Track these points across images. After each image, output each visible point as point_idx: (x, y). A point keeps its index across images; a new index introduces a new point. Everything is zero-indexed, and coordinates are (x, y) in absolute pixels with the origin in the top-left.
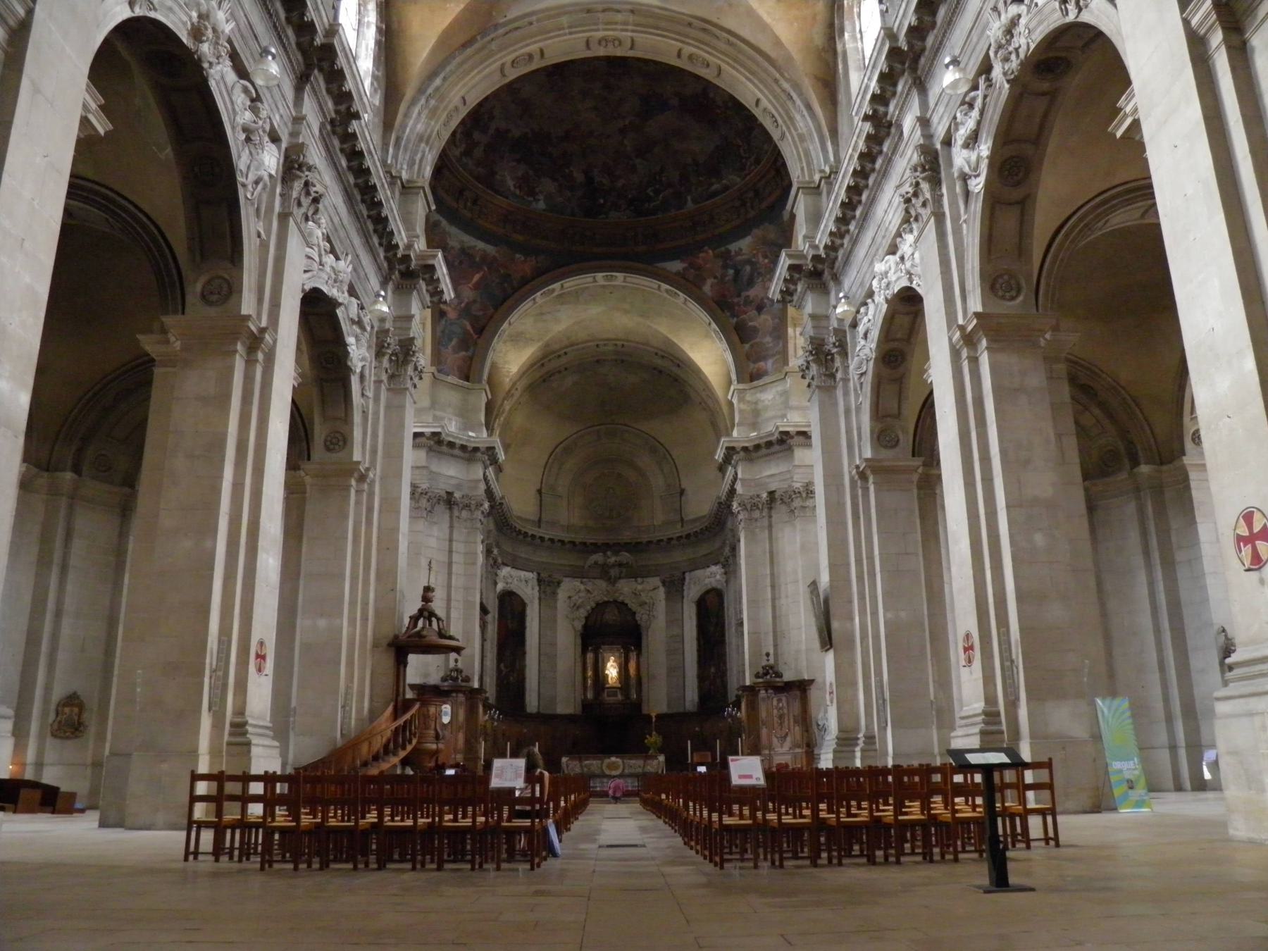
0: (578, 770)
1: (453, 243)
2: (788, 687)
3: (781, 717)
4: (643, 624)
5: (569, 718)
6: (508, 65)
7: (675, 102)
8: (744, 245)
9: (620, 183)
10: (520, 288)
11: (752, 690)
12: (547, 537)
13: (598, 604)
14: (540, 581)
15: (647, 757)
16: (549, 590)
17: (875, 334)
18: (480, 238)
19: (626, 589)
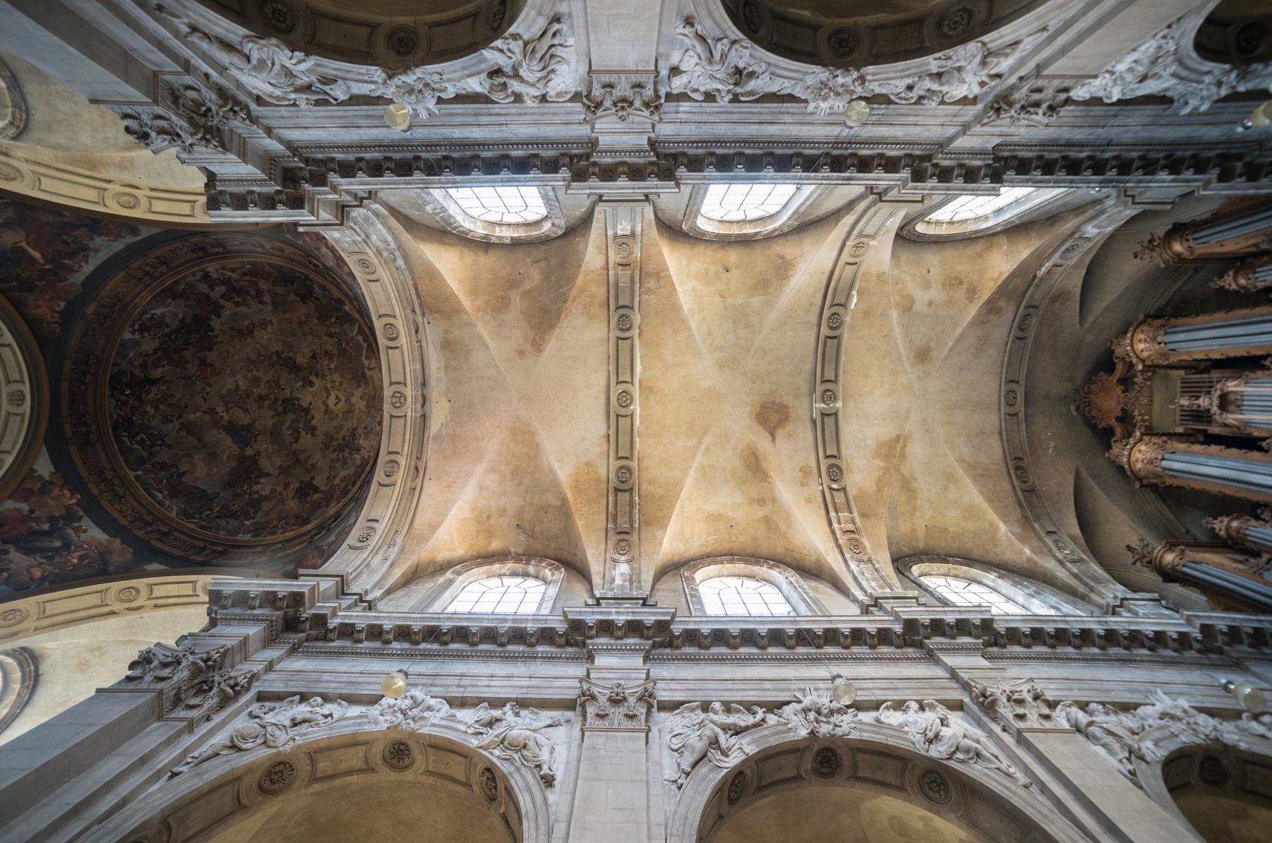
1: (98, 241)
6: (391, 320)
7: (249, 452)
8: (94, 534)
9: (150, 410)
10: (9, 299)
17: (316, 734)
18: (99, 269)
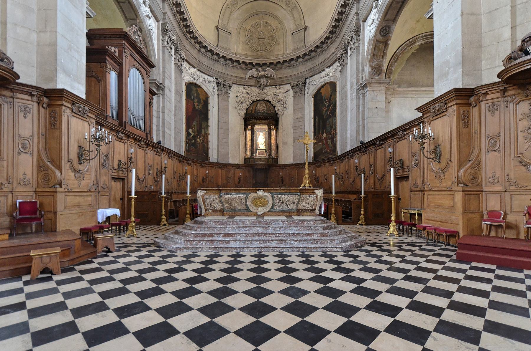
0: (218, 206)
4: (279, 113)
5: (237, 166)
12: (221, 55)
13: (253, 102)
14: (218, 84)
15: (302, 191)
16: (224, 90)
19: (270, 93)
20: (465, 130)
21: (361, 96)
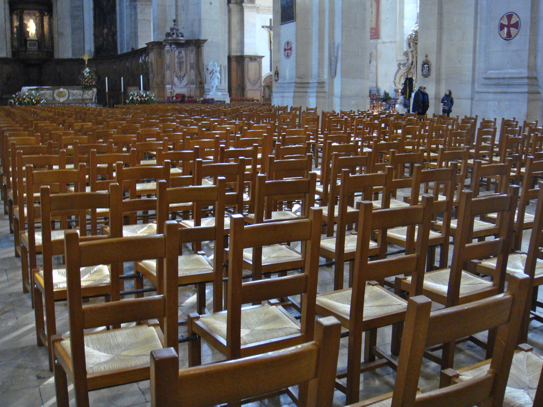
2: (188, 43)
3: (181, 63)
11: (158, 45)
20: (159, 60)
21: (133, 7)
